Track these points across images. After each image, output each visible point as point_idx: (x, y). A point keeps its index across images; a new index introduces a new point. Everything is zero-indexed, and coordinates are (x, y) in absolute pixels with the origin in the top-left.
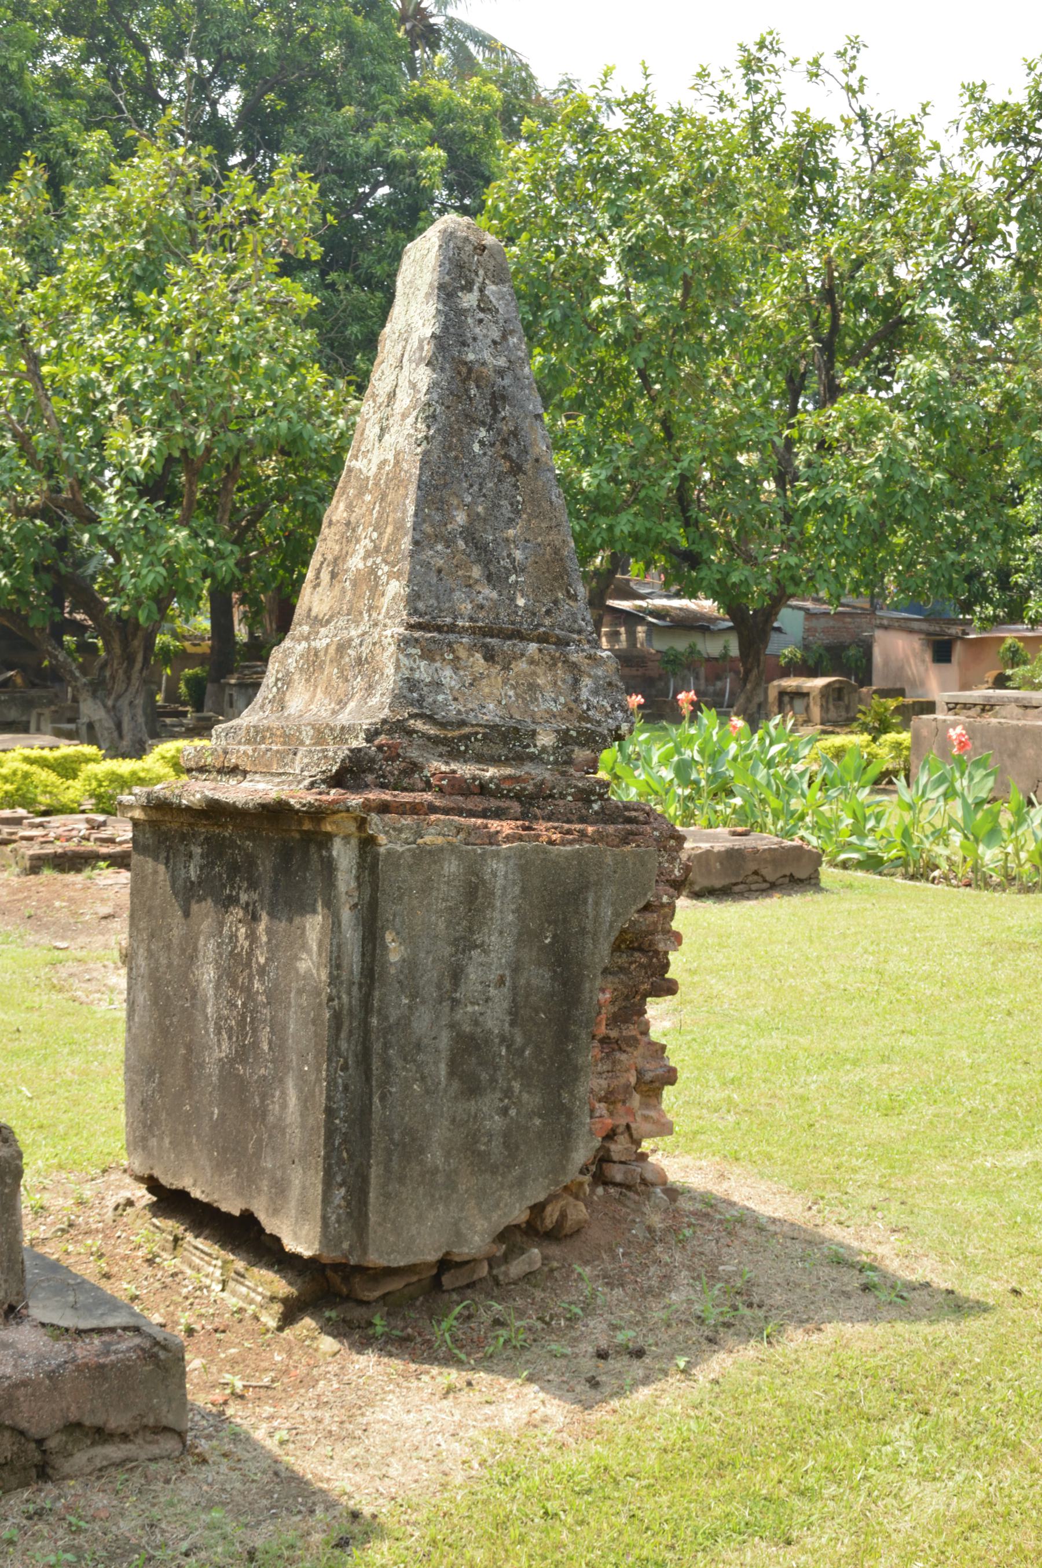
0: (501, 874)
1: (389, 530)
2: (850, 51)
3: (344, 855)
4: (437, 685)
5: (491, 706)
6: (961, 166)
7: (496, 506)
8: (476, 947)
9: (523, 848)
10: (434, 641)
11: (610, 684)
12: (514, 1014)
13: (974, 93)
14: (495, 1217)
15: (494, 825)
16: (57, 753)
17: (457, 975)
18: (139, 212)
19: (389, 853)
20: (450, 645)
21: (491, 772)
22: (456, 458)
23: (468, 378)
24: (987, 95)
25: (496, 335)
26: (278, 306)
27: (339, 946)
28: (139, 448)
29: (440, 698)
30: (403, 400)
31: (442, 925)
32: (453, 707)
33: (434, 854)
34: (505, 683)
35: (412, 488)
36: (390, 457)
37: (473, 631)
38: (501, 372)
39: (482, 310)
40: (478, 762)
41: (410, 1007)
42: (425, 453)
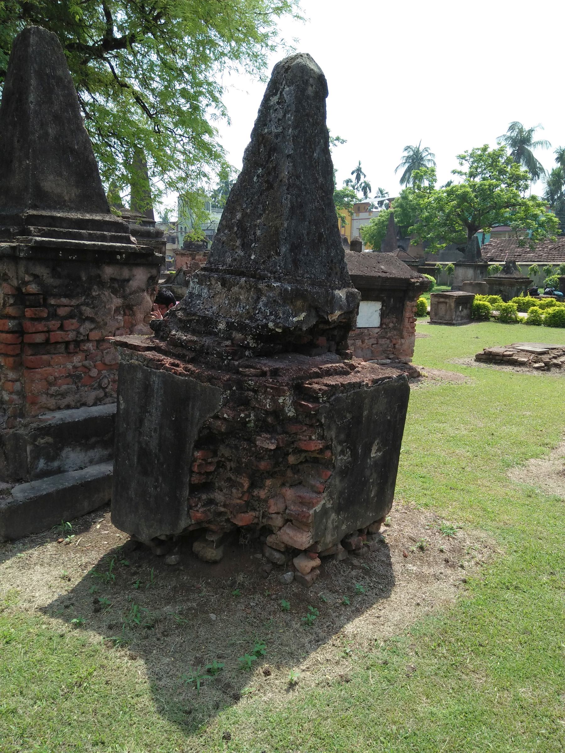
4: (200, 296)
7: (256, 208)
8: (148, 412)
11: (275, 301)
17: (141, 421)
20: (209, 278)
22: (245, 186)
25: (280, 116)
31: (137, 399)
33: (132, 367)
34: (226, 297)
38: (277, 136)
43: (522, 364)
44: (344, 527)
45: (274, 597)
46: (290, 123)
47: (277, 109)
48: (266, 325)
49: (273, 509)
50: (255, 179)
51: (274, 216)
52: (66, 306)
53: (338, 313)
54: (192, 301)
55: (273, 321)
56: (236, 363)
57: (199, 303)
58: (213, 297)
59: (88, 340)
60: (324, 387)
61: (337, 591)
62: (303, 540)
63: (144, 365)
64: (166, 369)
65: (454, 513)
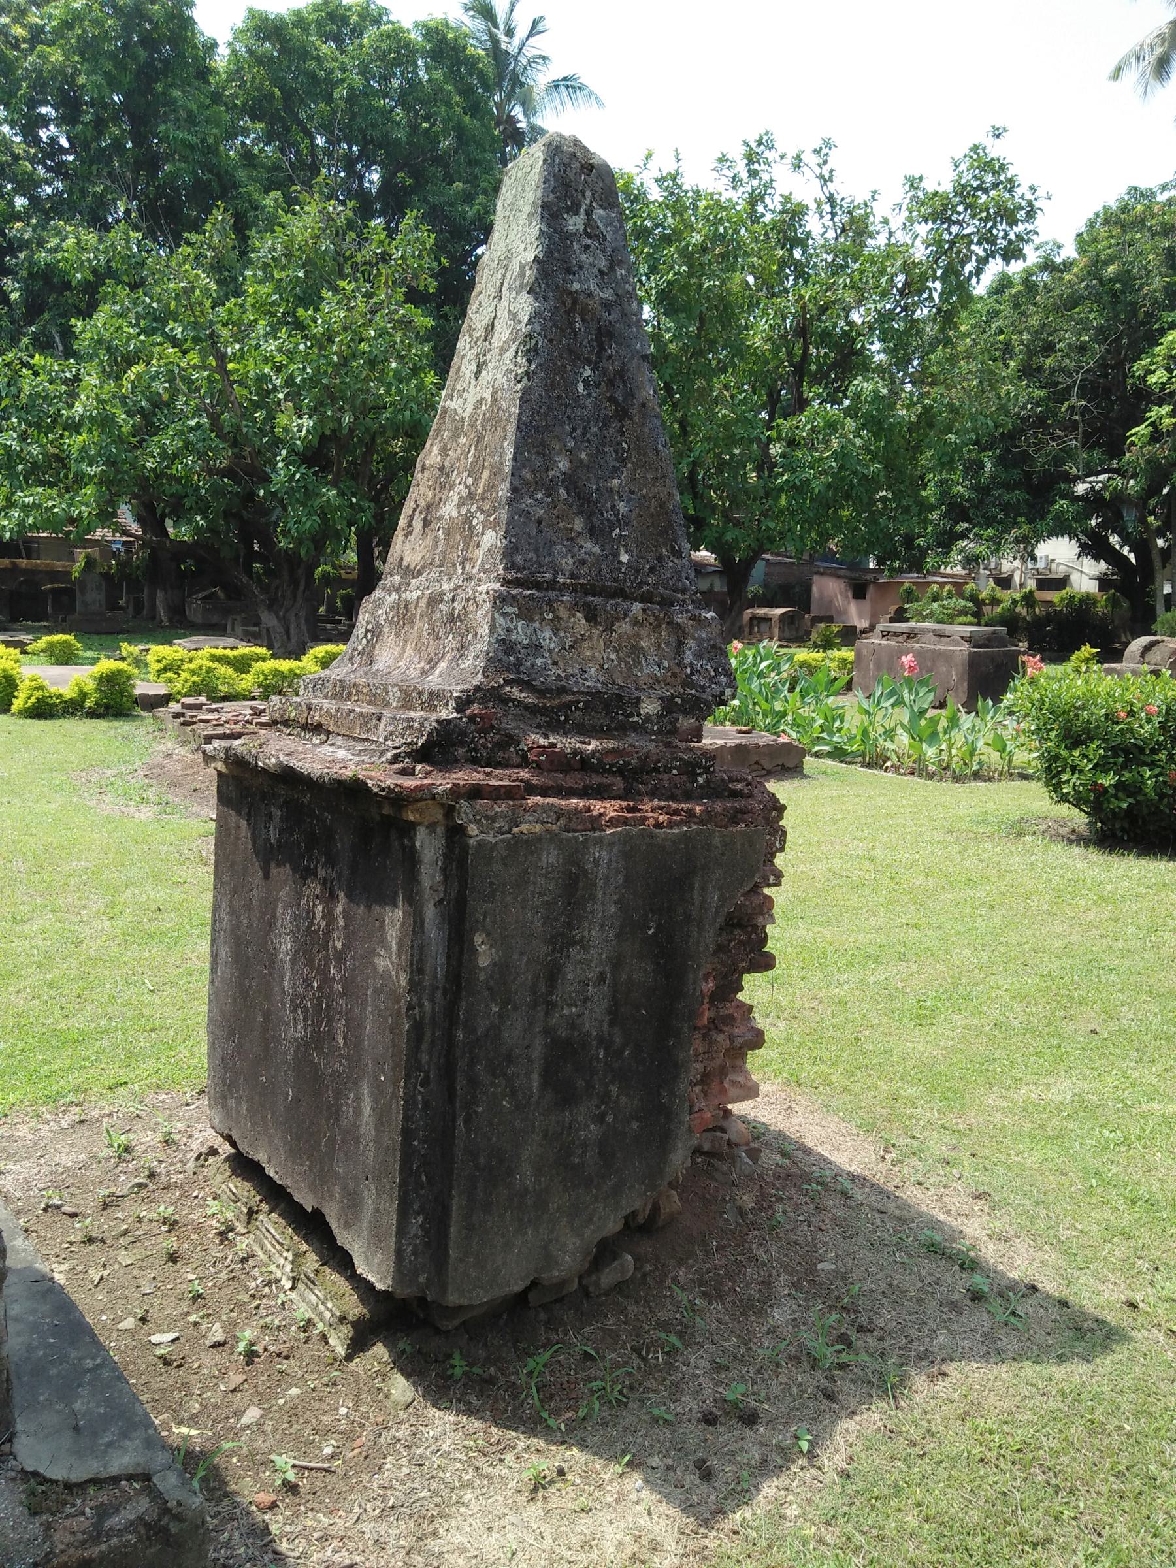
0: (604, 862)
1: (486, 475)
2: (824, 150)
3: (429, 847)
4: (536, 647)
5: (593, 671)
6: (901, 237)
7: (600, 453)
8: (574, 943)
9: (628, 832)
11: (714, 646)
12: (614, 1014)
13: (913, 183)
14: (588, 1233)
15: (597, 806)
16: (236, 653)
17: (553, 975)
18: (300, 248)
19: (480, 844)
21: (593, 745)
22: (559, 397)
23: (572, 310)
24: (922, 185)
25: (603, 264)
26: (405, 324)
27: (421, 948)
28: (299, 426)
29: (539, 661)
30: (502, 333)
31: (538, 923)
32: (553, 671)
33: (531, 844)
34: (607, 646)
35: (511, 429)
36: (487, 395)
37: (574, 589)
38: (607, 306)
39: (589, 236)
40: (580, 733)
41: (500, 1016)
42: (525, 390)
51: (649, 476)
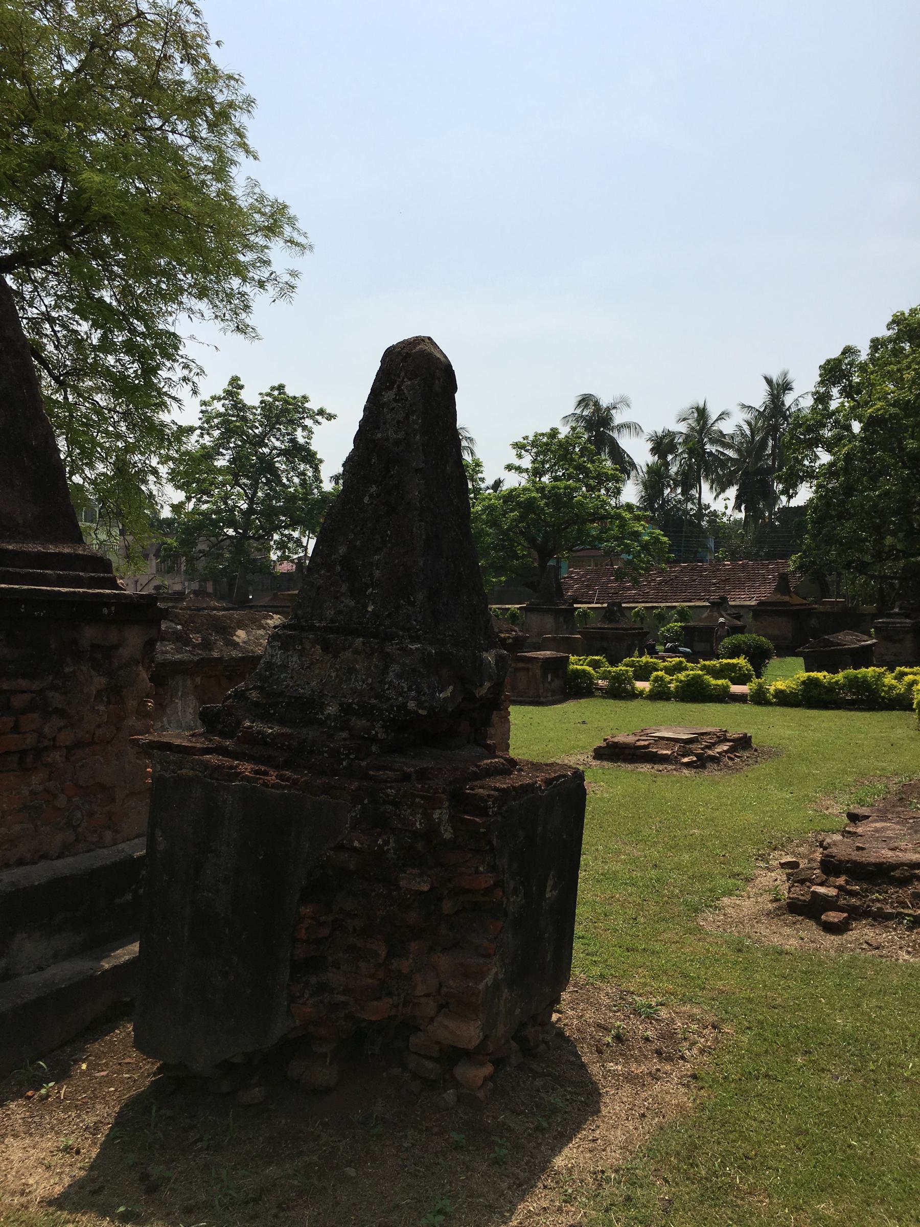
4: (284, 667)
10: (290, 636)
34: (331, 667)
38: (397, 443)
43: (664, 759)
44: (518, 1011)
45: (435, 1130)
46: (416, 427)
47: (393, 408)
48: (404, 706)
49: (420, 990)
50: (366, 500)
52: (25, 692)
53: (487, 685)
54: (271, 675)
55: (414, 699)
56: (364, 764)
57: (286, 677)
58: (308, 667)
59: (55, 747)
60: (492, 792)
61: (522, 1112)
62: (469, 1033)
63: (205, 776)
64: (247, 779)
65: (645, 984)
